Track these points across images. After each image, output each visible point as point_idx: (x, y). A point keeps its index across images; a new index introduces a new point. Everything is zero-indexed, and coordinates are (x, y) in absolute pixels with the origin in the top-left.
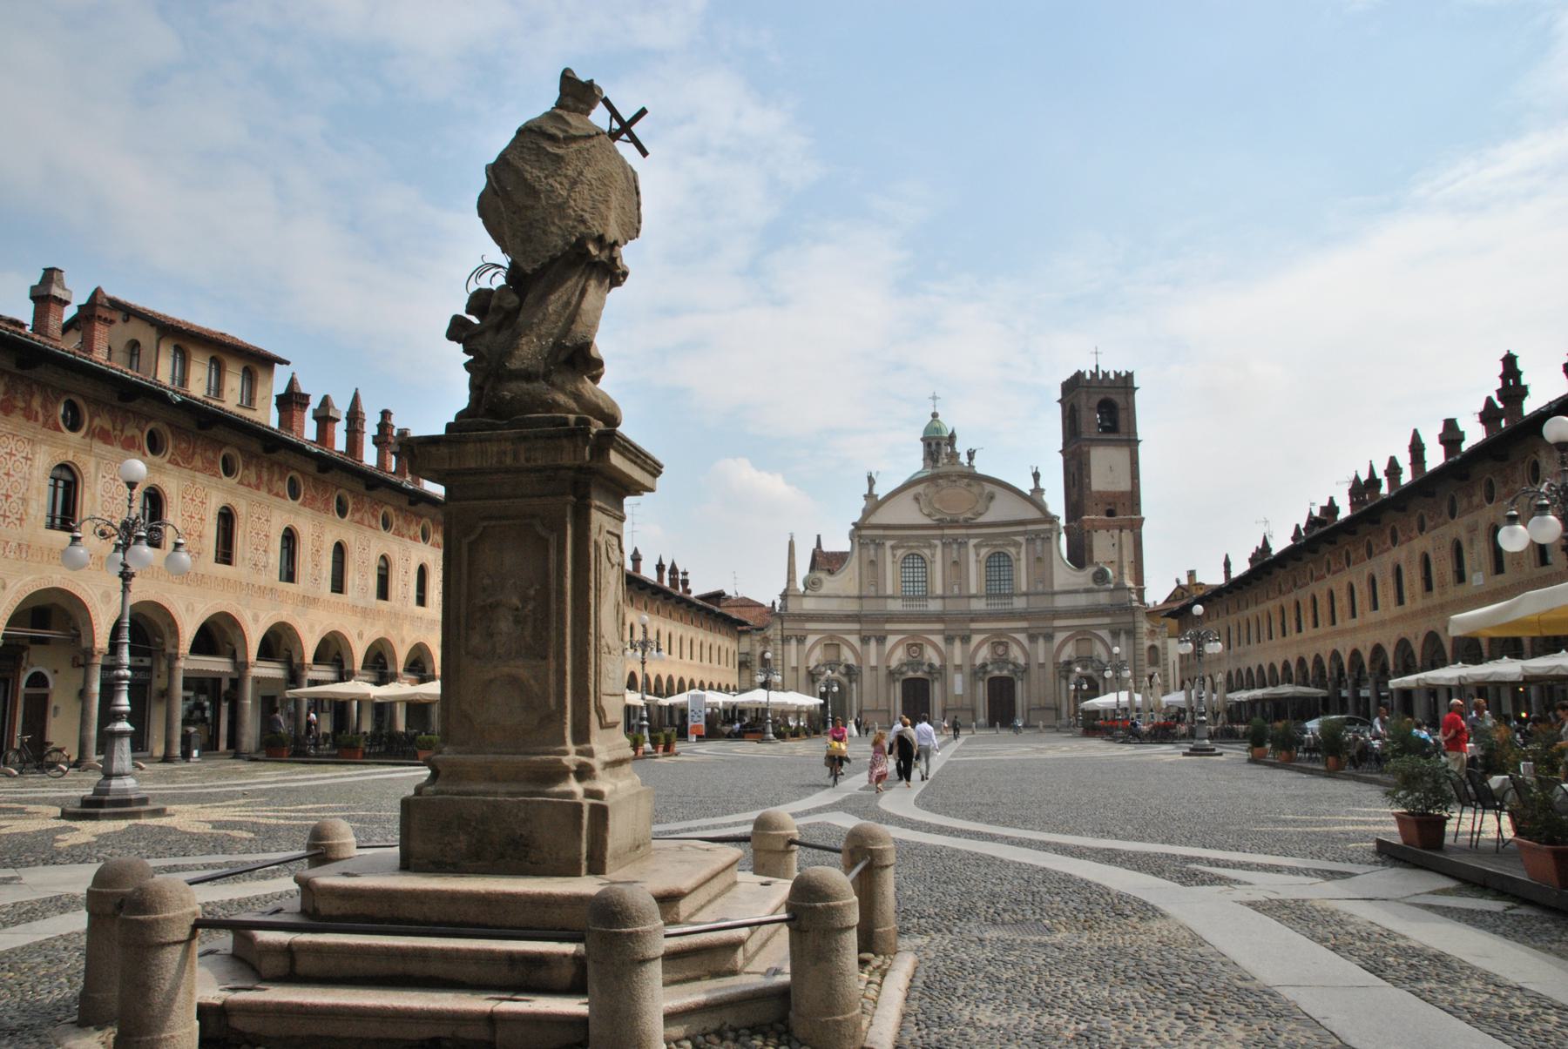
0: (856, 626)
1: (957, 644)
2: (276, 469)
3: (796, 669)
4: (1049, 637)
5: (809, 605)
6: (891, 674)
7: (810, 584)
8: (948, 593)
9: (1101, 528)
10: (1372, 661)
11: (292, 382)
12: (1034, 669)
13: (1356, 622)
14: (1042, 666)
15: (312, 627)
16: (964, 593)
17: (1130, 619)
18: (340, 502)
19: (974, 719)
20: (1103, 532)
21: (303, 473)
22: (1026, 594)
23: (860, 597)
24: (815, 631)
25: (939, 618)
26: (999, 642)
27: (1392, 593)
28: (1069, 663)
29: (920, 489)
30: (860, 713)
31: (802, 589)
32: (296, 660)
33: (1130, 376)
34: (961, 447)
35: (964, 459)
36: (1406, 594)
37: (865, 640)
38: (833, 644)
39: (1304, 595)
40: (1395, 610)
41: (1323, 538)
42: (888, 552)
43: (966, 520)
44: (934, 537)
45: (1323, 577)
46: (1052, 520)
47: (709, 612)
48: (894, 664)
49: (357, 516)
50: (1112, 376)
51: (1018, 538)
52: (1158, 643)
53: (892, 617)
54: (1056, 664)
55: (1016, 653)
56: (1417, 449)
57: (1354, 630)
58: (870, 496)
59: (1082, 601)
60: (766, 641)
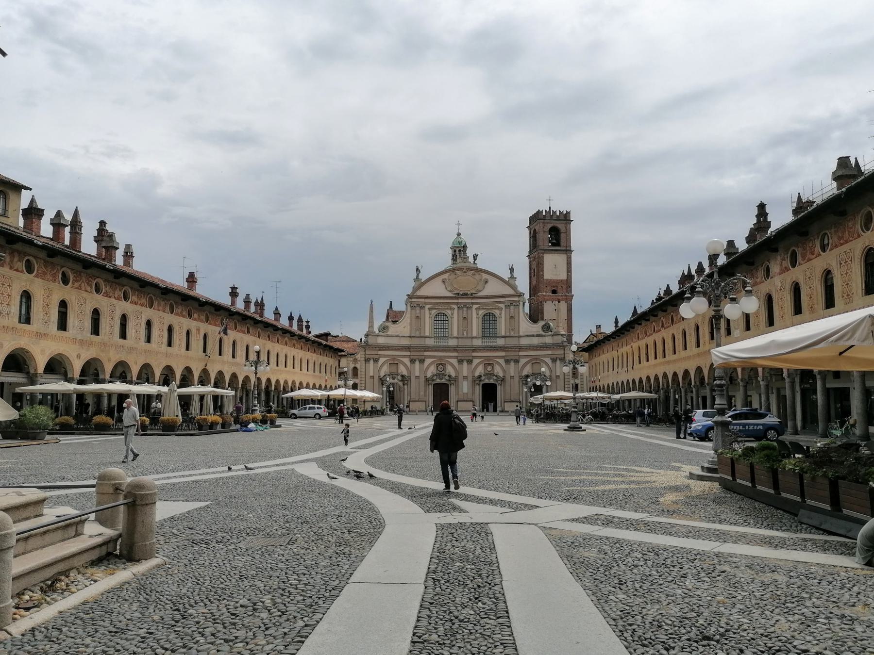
0: (408, 353)
1: (465, 363)
2: (16, 254)
3: (372, 377)
4: (517, 361)
5: (381, 341)
6: (427, 380)
7: (383, 328)
10: (684, 379)
11: (33, 201)
12: (508, 378)
14: (512, 377)
15: (43, 352)
16: (469, 335)
18: (64, 274)
20: (549, 303)
21: (35, 257)
23: (410, 337)
24: (385, 356)
25: (455, 349)
28: (527, 376)
29: (446, 276)
31: (377, 332)
32: (32, 371)
33: (568, 213)
34: (470, 253)
35: (471, 260)
37: (413, 361)
38: (394, 363)
42: (427, 312)
43: (472, 294)
46: (520, 295)
47: (320, 344)
48: (429, 375)
49: (77, 285)
50: (558, 214)
53: (427, 349)
54: (520, 377)
58: (417, 279)
59: (536, 341)
60: (356, 360)
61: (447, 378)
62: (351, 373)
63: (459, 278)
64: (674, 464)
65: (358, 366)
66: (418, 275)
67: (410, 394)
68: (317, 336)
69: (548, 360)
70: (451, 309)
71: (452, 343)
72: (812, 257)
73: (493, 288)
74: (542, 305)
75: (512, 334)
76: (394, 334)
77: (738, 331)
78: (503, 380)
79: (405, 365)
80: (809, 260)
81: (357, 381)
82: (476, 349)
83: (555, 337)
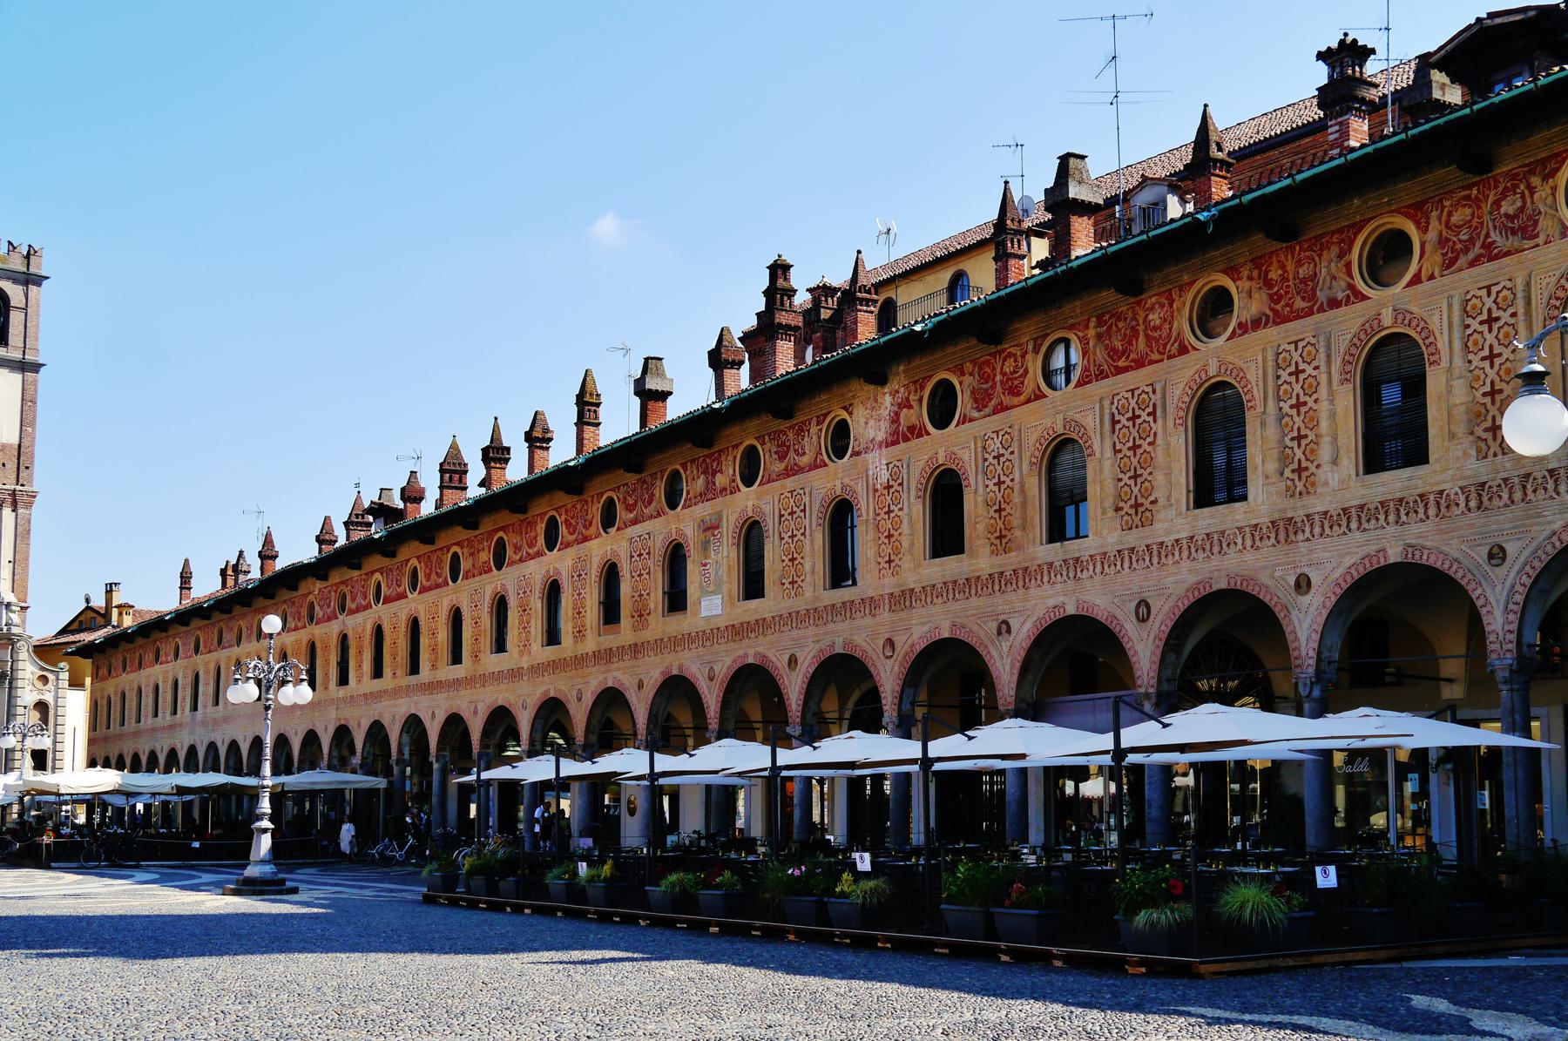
13: (459, 671)
27: (537, 626)
36: (566, 626)
39: (358, 624)
40: (541, 653)
41: (386, 541)
45: (402, 596)
52: (49, 698)
56: (587, 405)
57: (456, 683)
64: (1419, 1001)
72: (1007, 400)
77: (717, 600)
80: (1001, 408)
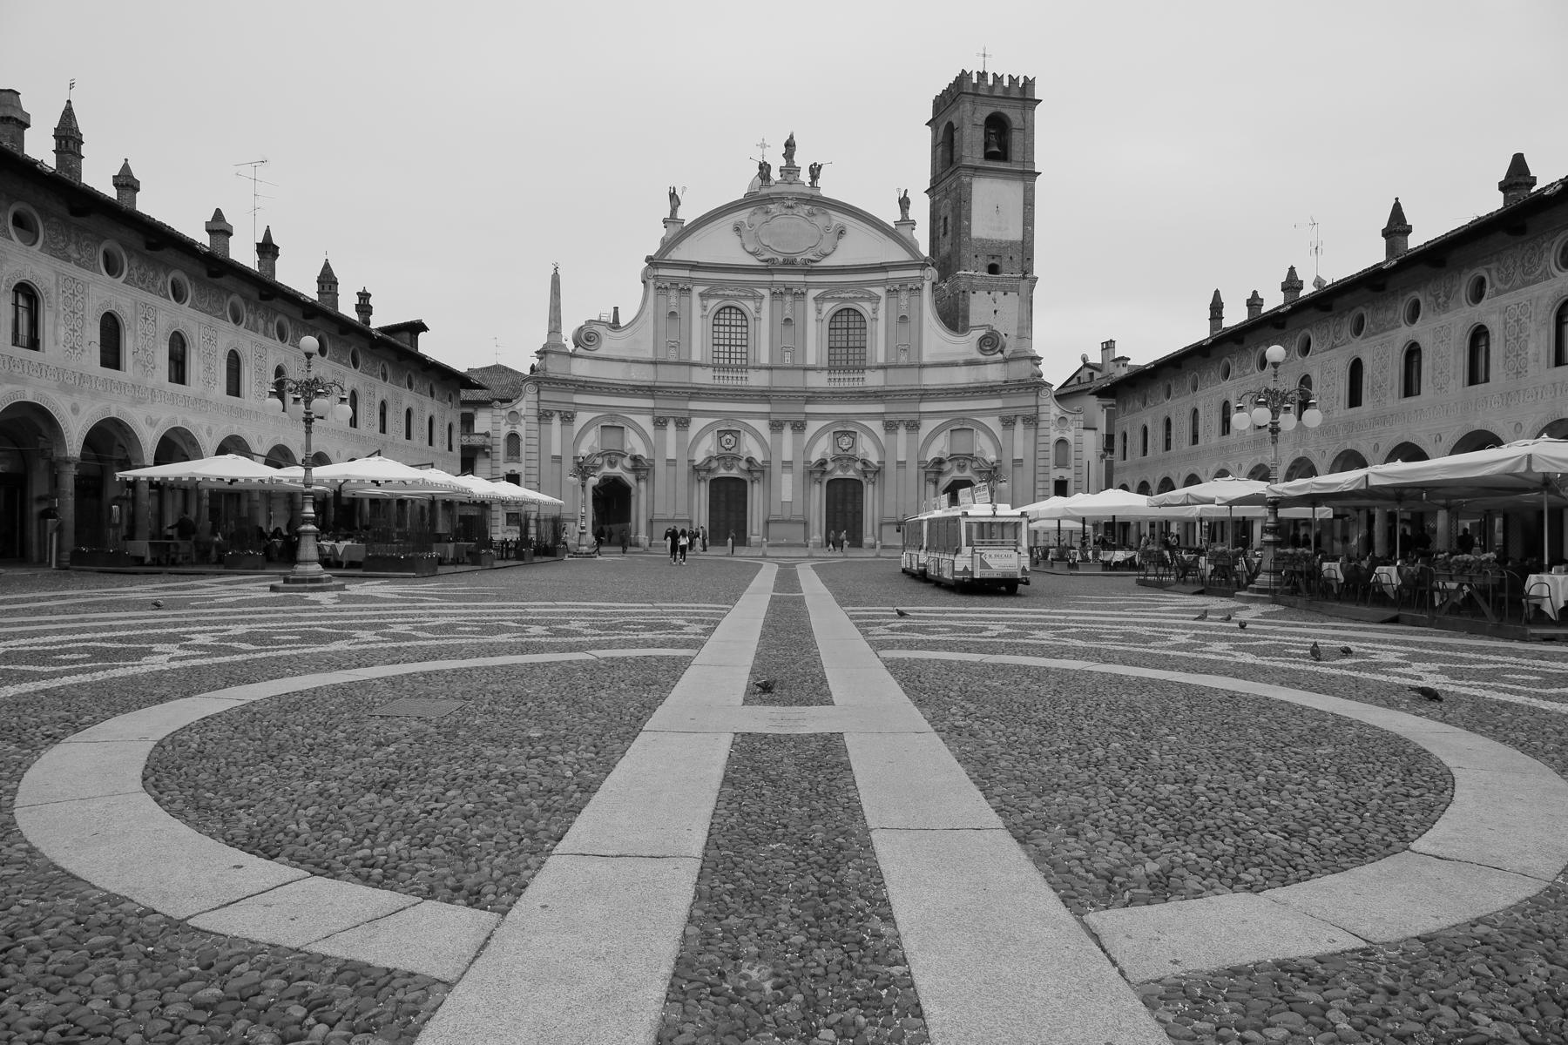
0: (649, 403)
1: (787, 432)
4: (913, 426)
5: (581, 369)
6: (696, 469)
8: (777, 363)
9: (982, 288)
12: (890, 467)
16: (799, 362)
17: (1031, 401)
19: (807, 537)
20: (982, 294)
22: (883, 368)
23: (654, 363)
25: (764, 395)
26: (844, 431)
28: (939, 462)
29: (743, 216)
30: (651, 522)
31: (570, 346)
33: (1029, 84)
34: (802, 160)
35: (805, 177)
37: (660, 423)
38: (613, 426)
42: (696, 301)
44: (761, 284)
48: (700, 458)
50: (1006, 83)
51: (880, 291)
53: (697, 393)
54: (922, 464)
55: (867, 449)
58: (671, 220)
59: (962, 377)
61: (743, 465)
62: (502, 448)
63: (775, 222)
65: (521, 430)
66: (674, 211)
67: (651, 501)
68: (380, 329)
69: (993, 423)
70: (754, 298)
71: (758, 380)
73: (859, 247)
74: (966, 300)
75: (903, 359)
76: (613, 354)
78: (878, 471)
79: (642, 433)
81: (517, 468)
82: (813, 397)
83: (1014, 366)
